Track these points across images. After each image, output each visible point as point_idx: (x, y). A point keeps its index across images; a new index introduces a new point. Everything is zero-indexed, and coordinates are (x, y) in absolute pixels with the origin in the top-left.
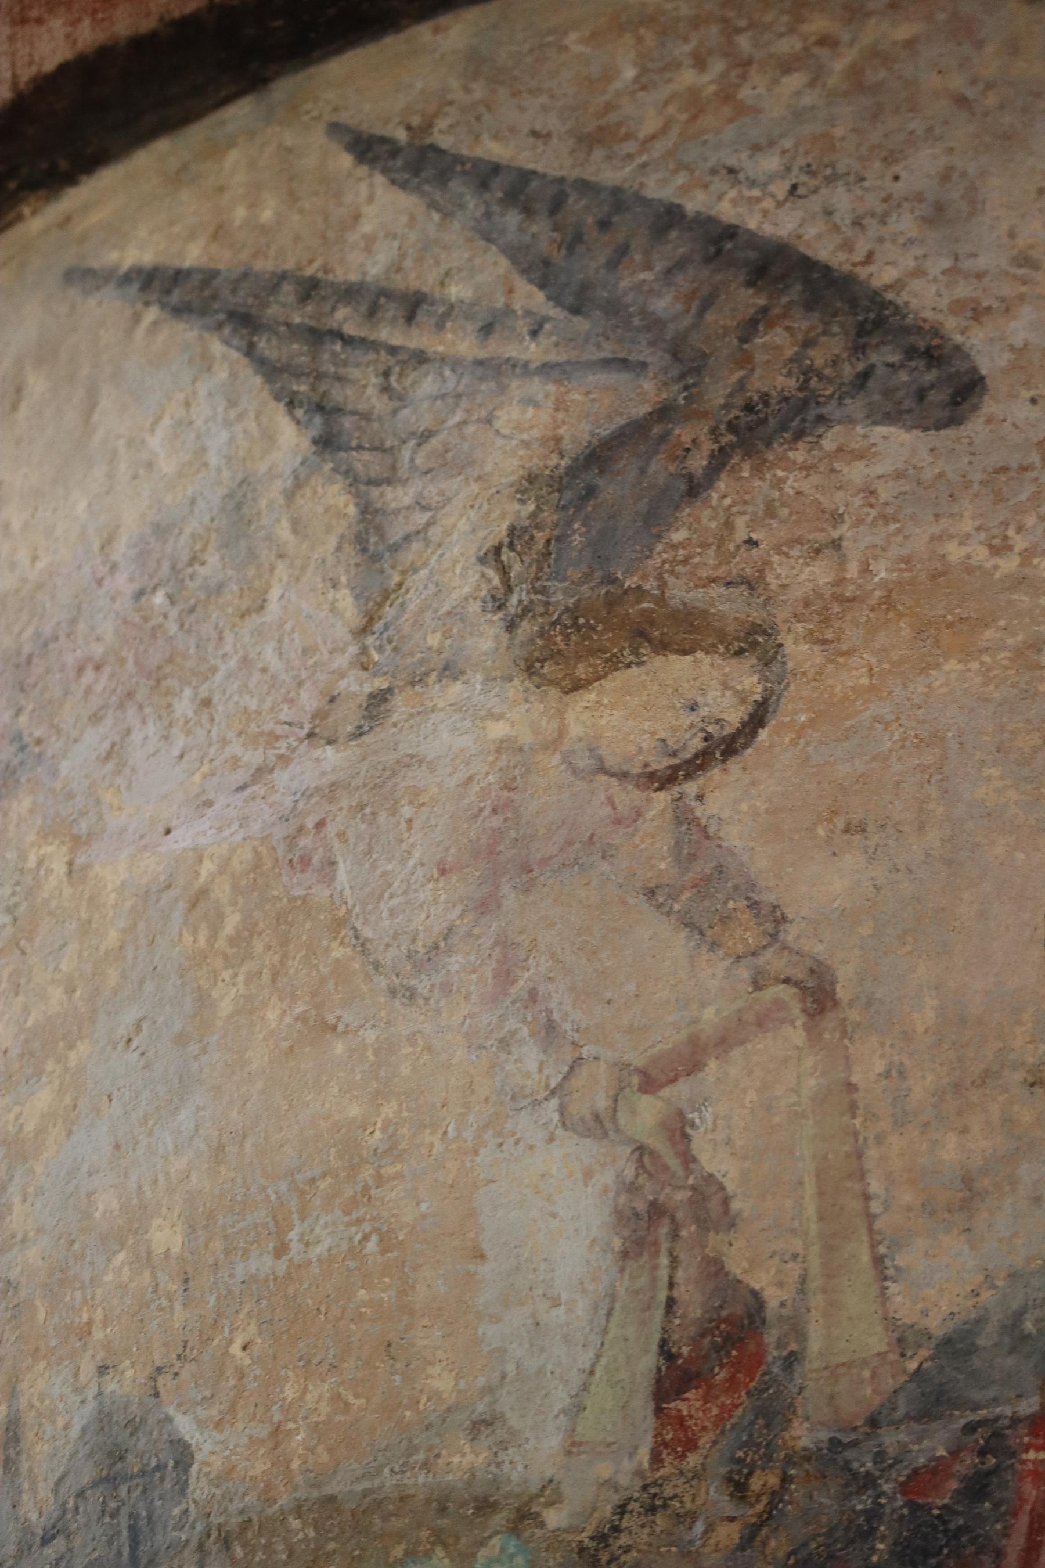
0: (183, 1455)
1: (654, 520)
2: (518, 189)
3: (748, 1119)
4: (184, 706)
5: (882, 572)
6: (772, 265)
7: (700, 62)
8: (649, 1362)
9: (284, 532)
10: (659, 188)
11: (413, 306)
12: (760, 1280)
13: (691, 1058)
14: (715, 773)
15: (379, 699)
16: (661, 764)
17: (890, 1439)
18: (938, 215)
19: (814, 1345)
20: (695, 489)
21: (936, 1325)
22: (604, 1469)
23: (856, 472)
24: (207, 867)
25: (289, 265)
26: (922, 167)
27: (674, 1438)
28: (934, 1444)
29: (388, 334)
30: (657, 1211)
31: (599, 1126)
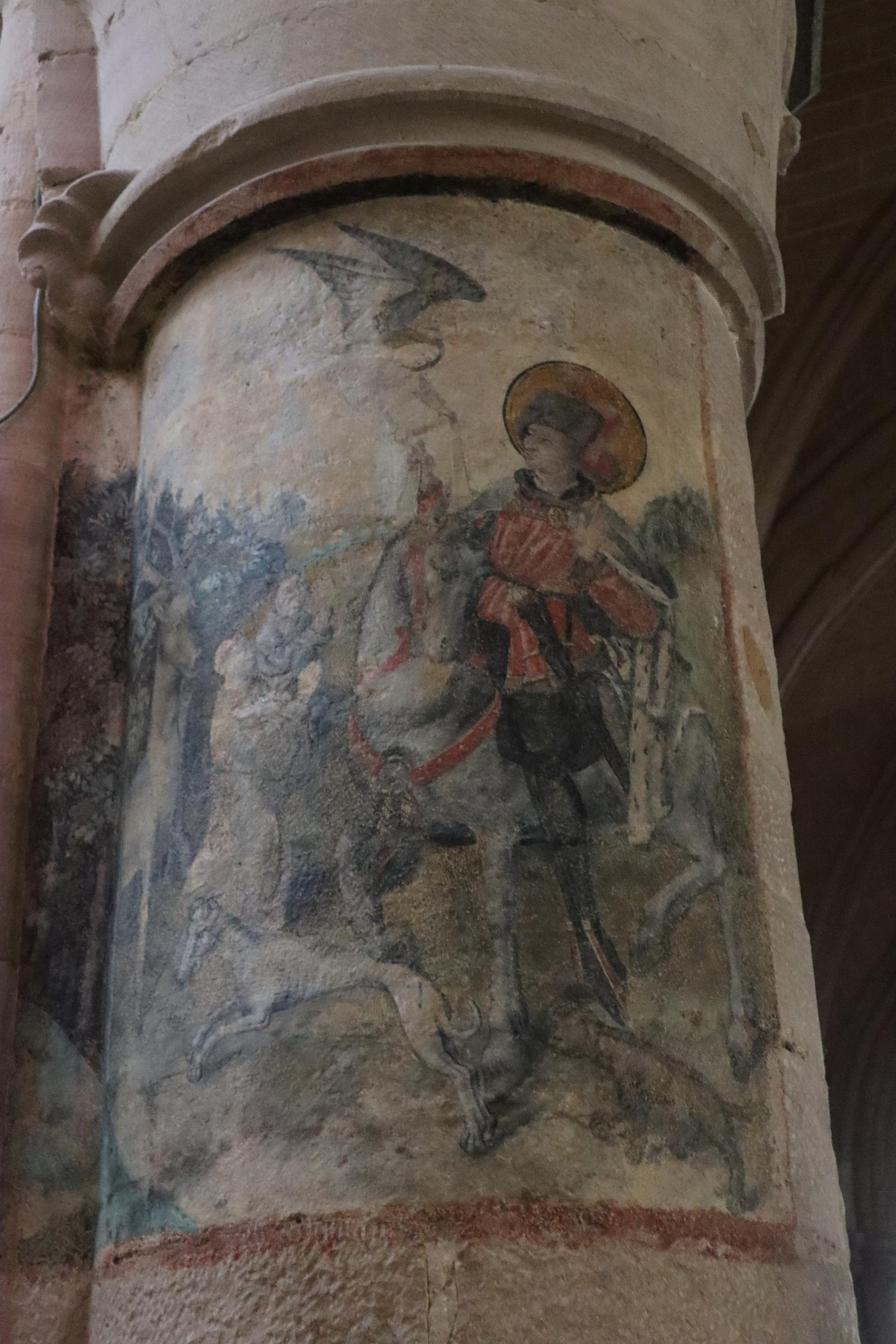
1: (414, 314)
2: (381, 240)
3: (437, 443)
4: (299, 343)
5: (465, 331)
6: (439, 263)
7: (421, 218)
8: (416, 492)
9: (324, 308)
10: (413, 244)
11: (355, 262)
12: (441, 478)
13: (425, 429)
14: (429, 369)
15: (348, 347)
16: (416, 366)
17: (470, 513)
18: (475, 257)
19: (454, 491)
20: (422, 308)
21: (480, 490)
22: (406, 513)
23: (459, 310)
24: (306, 379)
25: (324, 250)
26: (472, 246)
27: (422, 509)
28: (479, 515)
29: (349, 268)
30: (417, 461)
31: (403, 442)
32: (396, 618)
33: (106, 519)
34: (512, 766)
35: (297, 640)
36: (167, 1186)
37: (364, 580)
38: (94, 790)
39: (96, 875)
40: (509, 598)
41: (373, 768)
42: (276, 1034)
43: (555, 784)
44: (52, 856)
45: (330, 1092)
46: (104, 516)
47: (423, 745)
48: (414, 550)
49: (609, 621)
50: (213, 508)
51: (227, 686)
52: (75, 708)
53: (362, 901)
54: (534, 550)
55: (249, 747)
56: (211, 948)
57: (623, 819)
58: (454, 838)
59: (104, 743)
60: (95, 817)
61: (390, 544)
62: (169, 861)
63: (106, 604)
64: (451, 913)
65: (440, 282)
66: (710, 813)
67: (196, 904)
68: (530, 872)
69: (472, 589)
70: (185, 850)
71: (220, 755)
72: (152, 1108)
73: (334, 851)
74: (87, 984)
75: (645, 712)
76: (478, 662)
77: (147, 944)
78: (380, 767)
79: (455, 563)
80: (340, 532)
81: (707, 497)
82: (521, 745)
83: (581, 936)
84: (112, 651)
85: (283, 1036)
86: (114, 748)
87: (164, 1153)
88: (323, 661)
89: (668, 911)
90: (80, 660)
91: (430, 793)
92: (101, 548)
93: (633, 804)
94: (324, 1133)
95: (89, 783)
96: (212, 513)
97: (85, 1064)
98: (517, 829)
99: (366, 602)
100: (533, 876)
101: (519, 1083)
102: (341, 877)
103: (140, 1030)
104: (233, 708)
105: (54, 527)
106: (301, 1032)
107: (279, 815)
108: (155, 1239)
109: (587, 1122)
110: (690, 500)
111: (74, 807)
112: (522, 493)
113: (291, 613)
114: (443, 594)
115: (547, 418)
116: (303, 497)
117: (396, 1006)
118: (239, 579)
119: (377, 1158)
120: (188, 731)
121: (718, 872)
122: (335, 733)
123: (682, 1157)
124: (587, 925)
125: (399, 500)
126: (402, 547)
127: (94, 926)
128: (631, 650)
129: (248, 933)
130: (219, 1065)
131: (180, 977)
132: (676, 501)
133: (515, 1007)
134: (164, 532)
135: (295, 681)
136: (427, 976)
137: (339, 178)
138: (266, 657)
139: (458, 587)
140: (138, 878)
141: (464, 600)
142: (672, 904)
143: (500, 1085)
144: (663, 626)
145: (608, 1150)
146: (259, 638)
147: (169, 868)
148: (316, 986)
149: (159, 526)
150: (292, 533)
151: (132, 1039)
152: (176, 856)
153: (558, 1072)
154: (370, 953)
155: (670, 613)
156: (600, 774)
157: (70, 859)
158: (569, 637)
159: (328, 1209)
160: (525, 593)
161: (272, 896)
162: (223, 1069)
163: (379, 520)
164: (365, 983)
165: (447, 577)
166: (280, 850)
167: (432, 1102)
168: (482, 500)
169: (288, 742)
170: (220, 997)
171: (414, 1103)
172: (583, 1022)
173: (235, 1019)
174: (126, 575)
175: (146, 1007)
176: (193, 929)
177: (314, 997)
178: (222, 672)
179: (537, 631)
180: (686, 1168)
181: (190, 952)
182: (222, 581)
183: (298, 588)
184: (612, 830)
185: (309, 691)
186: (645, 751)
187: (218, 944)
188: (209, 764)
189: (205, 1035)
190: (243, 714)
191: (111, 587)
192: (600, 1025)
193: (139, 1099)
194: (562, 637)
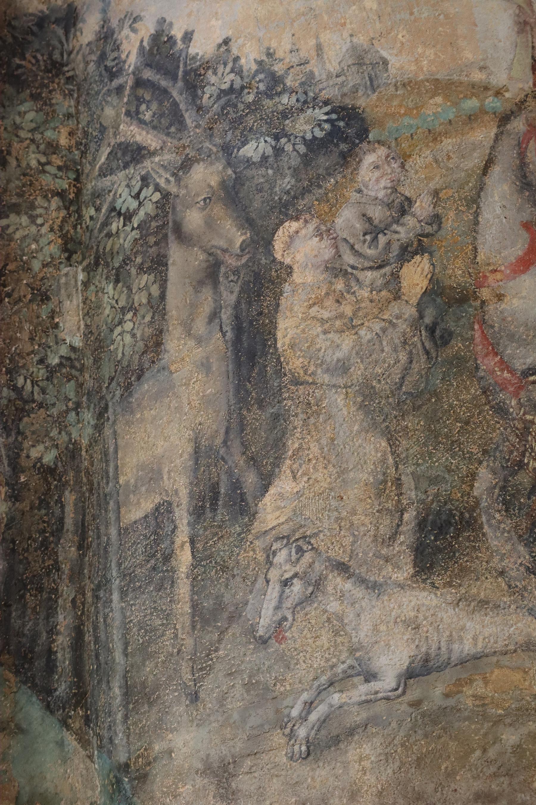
0: (385, 62)
22: (521, 86)
30: (526, 23)
32: (520, 210)
33: (38, 61)
35: (395, 227)
37: (476, 160)
38: (50, 399)
39: (63, 507)
41: (511, 389)
42: (416, 704)
45: (495, 775)
46: (35, 57)
50: (249, 56)
51: (297, 278)
52: (16, 295)
53: (514, 549)
55: (339, 355)
56: (307, 600)
60: (54, 433)
61: (504, 119)
62: (222, 491)
63: (48, 168)
70: (250, 479)
71: (295, 363)
73: (472, 486)
74: (62, 641)
77: (193, 592)
78: (520, 388)
80: (439, 100)
84: (61, 228)
86: (73, 348)
88: (431, 254)
90: (18, 235)
95: (43, 391)
96: (248, 63)
97: (71, 741)
99: (481, 188)
102: (484, 519)
103: (195, 698)
104: (310, 306)
106: (451, 702)
107: (392, 441)
111: (26, 419)
113: (381, 194)
116: (384, 54)
118: (302, 149)
120: (238, 330)
122: (457, 345)
125: (510, 69)
126: (518, 125)
127: (66, 568)
129: (363, 581)
130: (336, 741)
131: (261, 632)
135: (396, 276)
138: (352, 247)
140: (162, 513)
146: (339, 222)
147: (225, 500)
148: (467, 647)
150: (374, 97)
151: (179, 709)
152: (236, 486)
157: (26, 484)
161: (393, 537)
162: (342, 746)
163: (486, 88)
166: (398, 482)
169: (395, 350)
170: (327, 660)
173: (354, 686)
174: (70, 134)
176: (274, 574)
177: (462, 662)
178: (288, 261)
181: (274, 603)
182: (274, 148)
183: (389, 163)
185: (419, 291)
187: (319, 594)
188: (279, 372)
189: (309, 706)
190: (326, 315)
191: (53, 148)
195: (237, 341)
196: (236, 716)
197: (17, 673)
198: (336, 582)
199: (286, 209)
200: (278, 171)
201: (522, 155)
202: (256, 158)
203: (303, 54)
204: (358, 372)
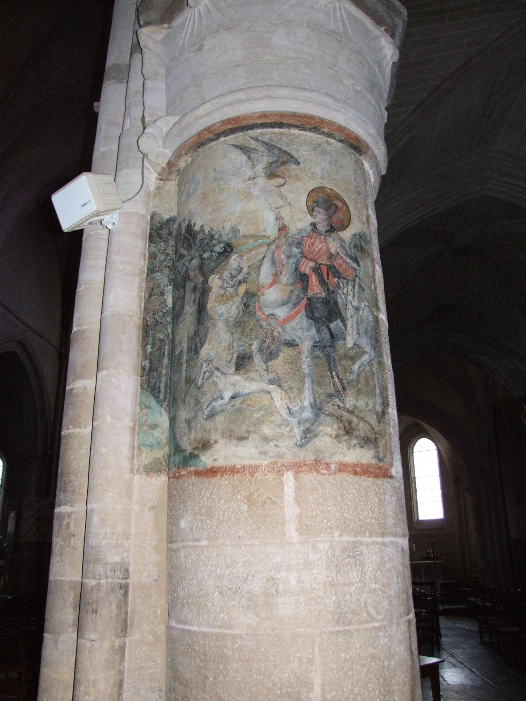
0: (239, 231)
1: (276, 168)
3: (285, 212)
6: (284, 152)
10: (275, 144)
11: (256, 150)
26: (295, 147)
31: (273, 211)
32: (271, 270)
34: (311, 321)
36: (196, 452)
37: (261, 256)
38: (163, 321)
40: (309, 265)
42: (233, 406)
43: (324, 327)
44: (150, 342)
47: (282, 313)
48: (278, 247)
49: (340, 274)
50: (207, 230)
54: (317, 249)
55: (221, 311)
56: (208, 378)
57: (344, 339)
58: (291, 344)
59: (167, 306)
60: (163, 330)
61: (269, 245)
64: (291, 369)
65: (285, 158)
66: (370, 337)
67: (204, 363)
68: (316, 356)
69: (297, 261)
72: (190, 428)
75: (351, 304)
76: (299, 286)
77: (186, 374)
79: (291, 252)
80: (252, 240)
81: (368, 233)
82: (313, 314)
83: (332, 377)
85: (235, 407)
87: (195, 442)
89: (358, 370)
90: (158, 278)
91: (284, 330)
92: (164, 241)
93: (347, 334)
94: (250, 438)
95: (162, 319)
96: (207, 232)
98: (312, 342)
100: (318, 357)
101: (313, 424)
103: (184, 403)
105: (148, 234)
107: (233, 335)
108: (193, 469)
109: (334, 436)
110: (363, 234)
112: (313, 230)
114: (288, 263)
115: (320, 205)
117: (273, 399)
118: (217, 255)
119: (267, 448)
120: (199, 304)
121: (373, 356)
123: (362, 447)
124: (334, 373)
126: (273, 247)
127: (164, 366)
128: (347, 284)
129: (222, 373)
132: (359, 235)
133: (312, 400)
134: (189, 237)
136: (283, 389)
137: (251, 122)
139: (292, 261)
140: (181, 352)
141: (294, 265)
142: (360, 367)
143: (307, 425)
144: (356, 276)
145: (341, 446)
146: (224, 275)
148: (246, 391)
149: (186, 235)
152: (196, 347)
153: (325, 421)
154: (264, 381)
155: (358, 272)
156: (338, 324)
158: (328, 279)
159: (252, 462)
160: (314, 263)
163: (265, 236)
164: (263, 391)
165: (289, 257)
167: (285, 430)
168: (300, 232)
171: (279, 431)
172: (333, 405)
175: (186, 395)
176: (202, 370)
179: (318, 276)
180: (364, 450)
184: (341, 343)
185: (243, 293)
186: (352, 317)
188: (207, 316)
189: (208, 405)
192: (338, 406)
193: (185, 424)
194: (326, 278)
195: (199, 307)
196: (192, 408)
197: (151, 393)
198: (216, 372)
199: (212, 272)
200: (211, 261)
201: (273, 255)
202: (206, 258)
203: (219, 229)
204: (225, 316)
